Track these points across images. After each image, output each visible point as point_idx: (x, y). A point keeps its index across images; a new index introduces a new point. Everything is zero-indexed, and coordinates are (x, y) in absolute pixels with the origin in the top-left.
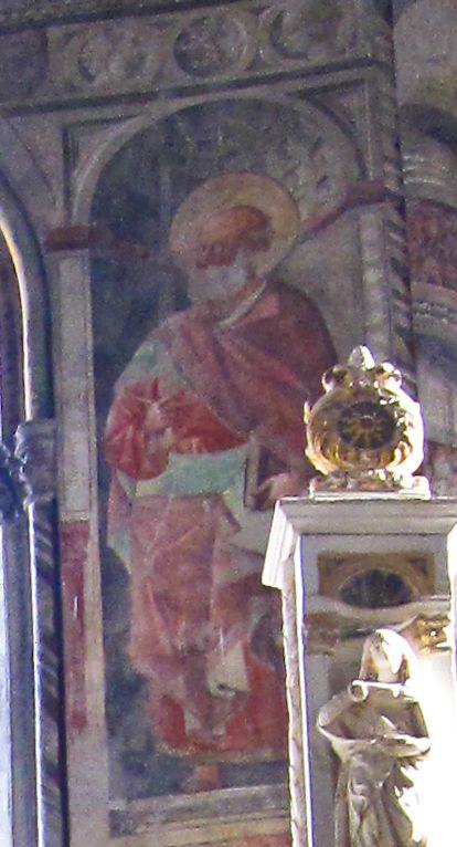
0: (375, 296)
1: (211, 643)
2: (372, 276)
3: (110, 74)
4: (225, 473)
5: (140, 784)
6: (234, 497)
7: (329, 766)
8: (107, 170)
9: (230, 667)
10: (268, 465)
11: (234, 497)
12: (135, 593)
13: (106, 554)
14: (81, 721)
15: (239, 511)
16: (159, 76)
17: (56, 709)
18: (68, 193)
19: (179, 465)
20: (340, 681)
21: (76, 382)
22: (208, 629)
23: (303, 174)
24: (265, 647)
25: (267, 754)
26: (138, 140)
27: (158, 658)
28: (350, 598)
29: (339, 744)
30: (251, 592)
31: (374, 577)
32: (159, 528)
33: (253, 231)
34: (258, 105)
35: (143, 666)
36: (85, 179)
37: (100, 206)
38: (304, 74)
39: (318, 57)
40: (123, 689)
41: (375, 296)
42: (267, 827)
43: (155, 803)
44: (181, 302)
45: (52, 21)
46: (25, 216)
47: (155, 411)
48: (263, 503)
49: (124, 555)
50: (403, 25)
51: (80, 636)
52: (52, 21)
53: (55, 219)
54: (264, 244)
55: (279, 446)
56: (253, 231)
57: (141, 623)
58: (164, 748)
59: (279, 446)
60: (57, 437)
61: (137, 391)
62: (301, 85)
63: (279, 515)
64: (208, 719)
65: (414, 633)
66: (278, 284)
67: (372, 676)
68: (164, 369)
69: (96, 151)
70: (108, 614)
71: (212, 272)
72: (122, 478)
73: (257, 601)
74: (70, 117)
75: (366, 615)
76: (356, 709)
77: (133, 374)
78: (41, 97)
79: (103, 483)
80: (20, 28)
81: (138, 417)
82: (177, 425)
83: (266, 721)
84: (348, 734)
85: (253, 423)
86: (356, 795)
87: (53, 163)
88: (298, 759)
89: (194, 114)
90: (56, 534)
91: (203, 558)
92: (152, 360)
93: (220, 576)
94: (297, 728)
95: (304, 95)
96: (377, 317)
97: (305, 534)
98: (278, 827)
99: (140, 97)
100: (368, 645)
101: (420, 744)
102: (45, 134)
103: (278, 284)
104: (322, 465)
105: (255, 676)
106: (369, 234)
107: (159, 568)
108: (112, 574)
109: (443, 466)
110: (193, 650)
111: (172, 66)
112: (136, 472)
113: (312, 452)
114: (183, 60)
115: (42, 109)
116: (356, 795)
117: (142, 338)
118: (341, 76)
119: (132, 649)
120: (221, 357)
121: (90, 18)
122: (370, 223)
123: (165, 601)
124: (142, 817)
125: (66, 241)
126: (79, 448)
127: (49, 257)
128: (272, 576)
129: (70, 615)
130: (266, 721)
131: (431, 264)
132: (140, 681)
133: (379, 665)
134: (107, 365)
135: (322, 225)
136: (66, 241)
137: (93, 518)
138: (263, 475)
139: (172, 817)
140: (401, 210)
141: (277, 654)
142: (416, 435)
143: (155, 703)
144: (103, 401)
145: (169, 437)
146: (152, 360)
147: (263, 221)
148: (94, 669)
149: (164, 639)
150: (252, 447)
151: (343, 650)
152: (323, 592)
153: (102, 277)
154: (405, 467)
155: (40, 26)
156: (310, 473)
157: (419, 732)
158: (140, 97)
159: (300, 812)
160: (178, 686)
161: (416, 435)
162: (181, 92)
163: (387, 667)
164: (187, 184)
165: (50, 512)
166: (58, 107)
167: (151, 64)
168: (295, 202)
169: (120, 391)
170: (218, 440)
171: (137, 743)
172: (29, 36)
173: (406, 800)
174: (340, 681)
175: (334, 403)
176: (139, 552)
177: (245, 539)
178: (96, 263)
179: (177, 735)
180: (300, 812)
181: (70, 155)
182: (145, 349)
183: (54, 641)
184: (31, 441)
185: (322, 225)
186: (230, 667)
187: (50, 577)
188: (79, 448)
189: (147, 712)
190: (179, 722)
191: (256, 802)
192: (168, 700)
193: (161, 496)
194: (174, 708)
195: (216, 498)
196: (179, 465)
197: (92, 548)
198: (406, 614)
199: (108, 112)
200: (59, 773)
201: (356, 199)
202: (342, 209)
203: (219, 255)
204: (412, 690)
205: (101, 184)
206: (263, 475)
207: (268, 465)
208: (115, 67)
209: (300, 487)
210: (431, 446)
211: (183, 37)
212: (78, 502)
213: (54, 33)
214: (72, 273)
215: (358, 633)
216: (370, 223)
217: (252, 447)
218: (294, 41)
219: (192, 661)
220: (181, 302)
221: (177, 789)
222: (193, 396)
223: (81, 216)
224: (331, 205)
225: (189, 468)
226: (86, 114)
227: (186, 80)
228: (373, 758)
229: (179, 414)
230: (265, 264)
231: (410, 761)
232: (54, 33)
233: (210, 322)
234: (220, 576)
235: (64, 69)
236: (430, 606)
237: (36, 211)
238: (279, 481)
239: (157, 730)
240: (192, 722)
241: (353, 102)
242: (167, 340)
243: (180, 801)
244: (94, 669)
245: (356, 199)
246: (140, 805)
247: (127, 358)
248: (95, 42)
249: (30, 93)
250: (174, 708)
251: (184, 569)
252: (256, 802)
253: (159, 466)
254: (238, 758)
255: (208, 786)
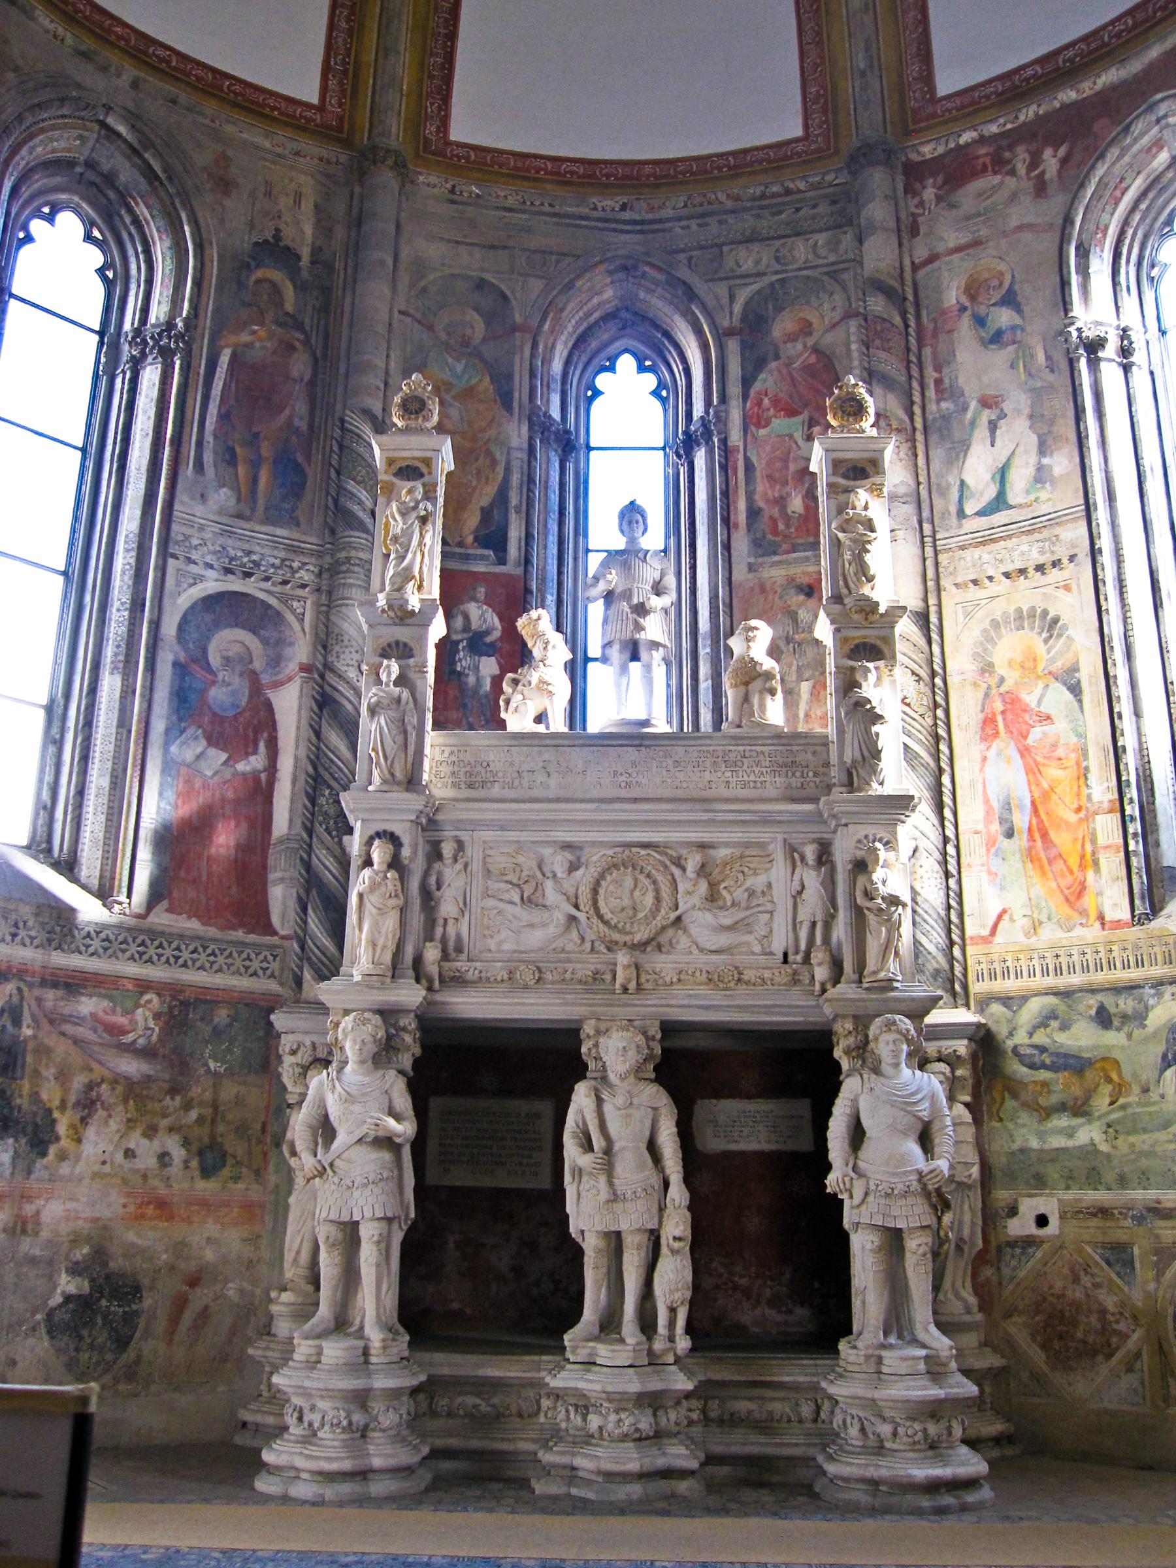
0: (855, 354)
1: (789, 494)
2: (854, 347)
3: (748, 265)
4: (794, 426)
5: (760, 552)
6: (798, 436)
7: (836, 544)
8: (747, 304)
9: (796, 504)
10: (812, 423)
11: (798, 436)
12: (758, 474)
13: (746, 459)
14: (736, 526)
15: (800, 442)
16: (768, 266)
17: (726, 521)
18: (731, 313)
19: (776, 422)
20: (841, 510)
21: (734, 390)
22: (788, 489)
23: (826, 306)
24: (811, 496)
25: (811, 539)
26: (759, 292)
27: (767, 501)
28: (845, 476)
29: (841, 535)
30: (805, 473)
31: (855, 468)
32: (768, 448)
33: (806, 328)
34: (808, 278)
35: (761, 504)
36: (738, 307)
37: (744, 319)
38: (827, 265)
39: (832, 258)
40: (753, 513)
41: (855, 354)
42: (811, 569)
43: (766, 559)
44: (777, 357)
45: (724, 244)
46: (714, 322)
47: (766, 401)
48: (810, 438)
49: (754, 459)
50: (867, 245)
51: (736, 492)
52: (724, 244)
53: (726, 323)
54: (810, 334)
55: (816, 415)
56: (806, 328)
57: (761, 487)
58: (770, 537)
59: (816, 415)
60: (727, 412)
61: (759, 393)
62: (825, 269)
63: (816, 443)
64: (788, 526)
65: (871, 490)
66: (816, 350)
67: (854, 508)
68: (770, 384)
69: (743, 296)
70: (747, 483)
71: (789, 345)
72: (753, 428)
73: (807, 478)
74: (732, 282)
75: (852, 483)
76: (847, 521)
77: (757, 386)
78: (721, 274)
79: (745, 430)
80: (712, 247)
81: (759, 403)
82: (775, 406)
83: (811, 526)
84: (844, 531)
85: (806, 406)
86: (847, 556)
87: (725, 301)
88: (824, 541)
89: (782, 281)
90: (727, 450)
91: (785, 460)
92: (765, 380)
93: (792, 467)
94: (824, 529)
95: (826, 274)
96: (856, 363)
97: (827, 451)
98: (815, 569)
99: (760, 275)
100: (852, 495)
101: (873, 535)
102: (722, 289)
103: (816, 350)
104: (833, 423)
105: (807, 508)
106: (853, 330)
107: (768, 464)
108: (749, 467)
109: (882, 423)
110: (781, 497)
111: (773, 262)
112: (759, 426)
113: (829, 418)
114: (777, 259)
115: (720, 279)
116: (847, 556)
117: (761, 371)
118: (841, 266)
119: (757, 497)
120: (793, 379)
121: (740, 243)
122: (853, 325)
123: (770, 478)
124: (761, 564)
125: (730, 332)
126: (735, 416)
127: (724, 339)
128: (813, 468)
129: (732, 483)
130: (811, 526)
131: (878, 342)
132: (760, 510)
133: (857, 503)
134: (747, 382)
135: (834, 326)
136: (730, 332)
137: (741, 444)
138: (810, 427)
139: (773, 564)
140: (866, 320)
141: (815, 499)
142: (871, 411)
143: (766, 519)
144: (745, 397)
145: (772, 412)
146: (765, 380)
147: (810, 324)
148: (742, 505)
149: (770, 493)
150: (805, 416)
151: (842, 498)
152: (834, 474)
153: (744, 346)
154: (867, 423)
155: (720, 246)
156: (829, 426)
157: (873, 530)
158: (760, 275)
159: (825, 562)
160: (775, 512)
161: (871, 411)
162: (777, 273)
163: (860, 504)
164: (779, 309)
165: (724, 441)
166: (727, 278)
167: (764, 261)
168: (823, 317)
169: (752, 393)
170: (792, 413)
171: (759, 535)
172: (715, 250)
173: (868, 558)
174: (841, 510)
175: (839, 398)
176: (760, 458)
177: (803, 453)
178: (742, 341)
179: (775, 531)
180: (825, 562)
181: (732, 298)
182: (762, 376)
183: (726, 494)
184: (716, 413)
185: (834, 326)
186: (796, 504)
187: (724, 468)
188: (735, 416)
189: (763, 523)
190: (776, 526)
191: (807, 559)
192: (771, 518)
193: (769, 435)
194: (774, 521)
195: (791, 436)
196: (776, 422)
197: (741, 456)
198: (868, 483)
199: (747, 280)
200: (727, 547)
201: (848, 315)
202: (842, 320)
203: (792, 338)
204: (870, 513)
205: (745, 310)
206: (810, 427)
207: (812, 423)
208: (750, 263)
209: (825, 432)
210: (878, 415)
211: (777, 250)
212: (735, 438)
213: (725, 249)
214: (733, 345)
215: (848, 491)
216: (853, 325)
217: (805, 416)
218: (822, 252)
219: (781, 502)
220: (777, 357)
221: (775, 553)
222: (781, 395)
223: (736, 322)
224: (838, 318)
225: (780, 424)
226: (738, 281)
227: (779, 267)
228: (854, 541)
229: (776, 402)
230: (810, 342)
231: (869, 542)
232: (725, 249)
233: (788, 365)
234: (792, 467)
235: (730, 263)
236: (877, 480)
237: (718, 321)
238: (816, 429)
239: (767, 530)
240: (781, 527)
241: (846, 276)
242: (771, 372)
243: (776, 558)
244: (742, 505)
245: (848, 315)
246: (760, 560)
247: (755, 379)
248: (742, 252)
249: (716, 272)
250: (774, 521)
251: (778, 465)
252: (807, 559)
253: (768, 423)
254: (800, 541)
255: (788, 552)
